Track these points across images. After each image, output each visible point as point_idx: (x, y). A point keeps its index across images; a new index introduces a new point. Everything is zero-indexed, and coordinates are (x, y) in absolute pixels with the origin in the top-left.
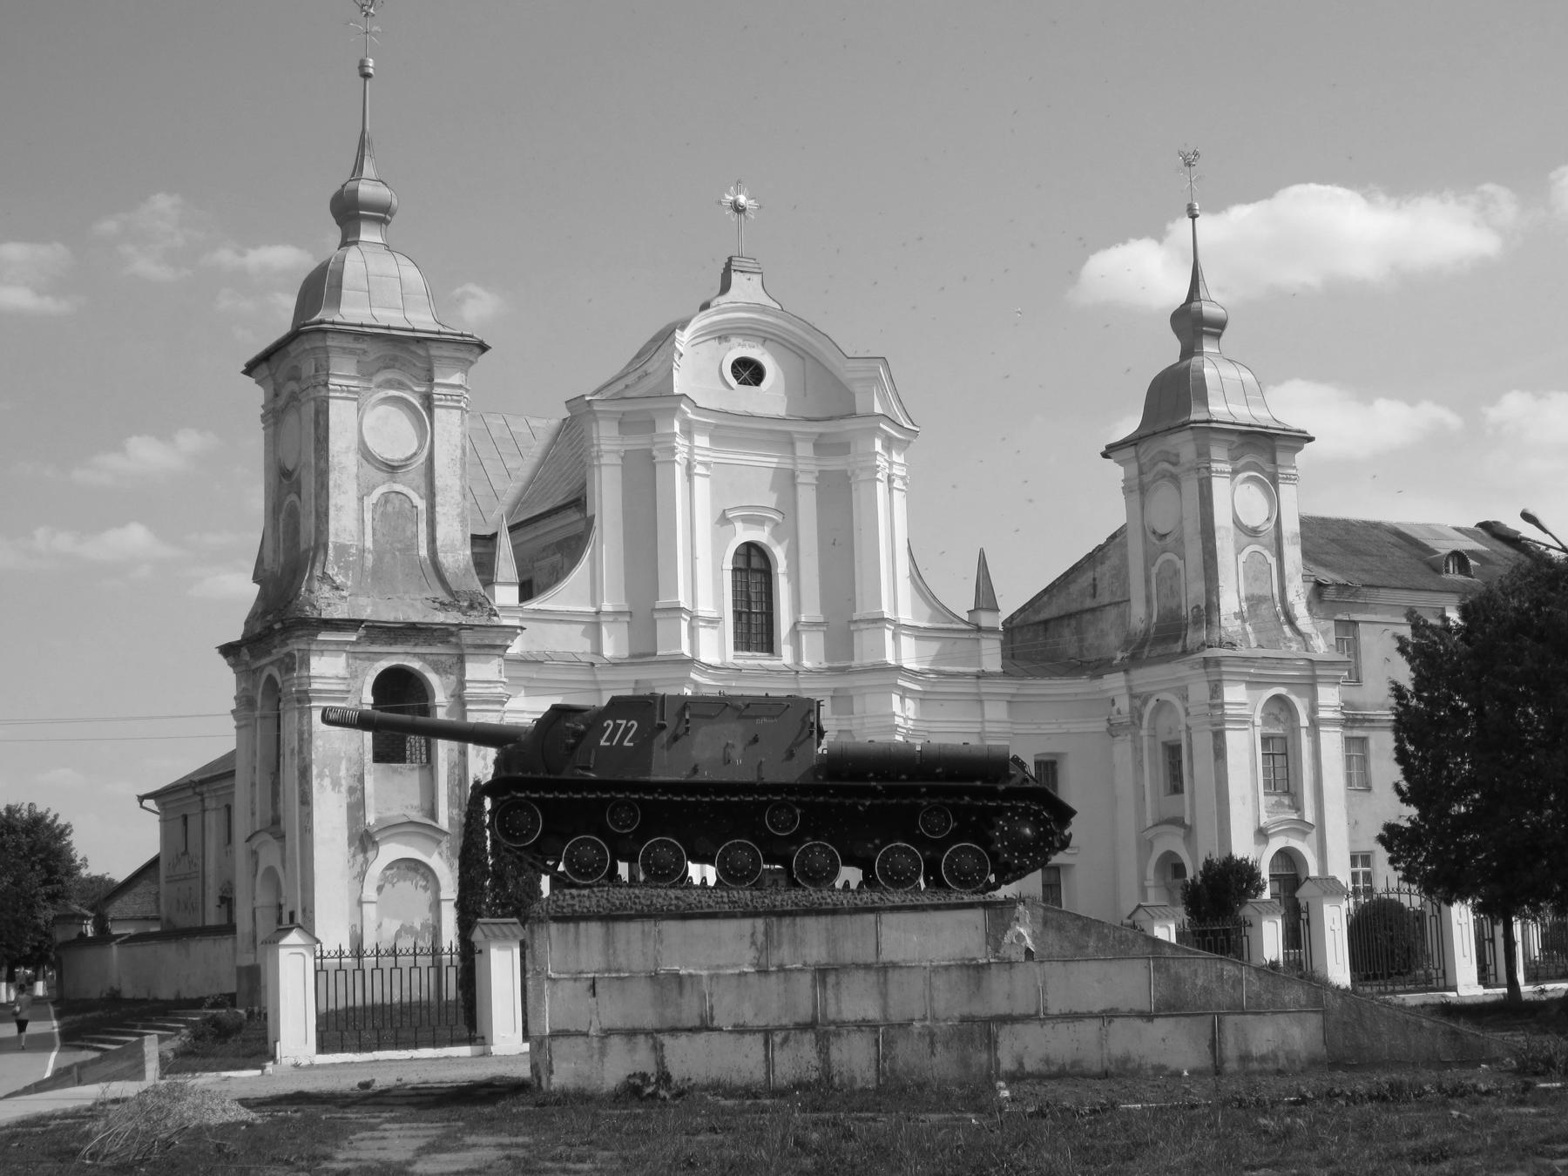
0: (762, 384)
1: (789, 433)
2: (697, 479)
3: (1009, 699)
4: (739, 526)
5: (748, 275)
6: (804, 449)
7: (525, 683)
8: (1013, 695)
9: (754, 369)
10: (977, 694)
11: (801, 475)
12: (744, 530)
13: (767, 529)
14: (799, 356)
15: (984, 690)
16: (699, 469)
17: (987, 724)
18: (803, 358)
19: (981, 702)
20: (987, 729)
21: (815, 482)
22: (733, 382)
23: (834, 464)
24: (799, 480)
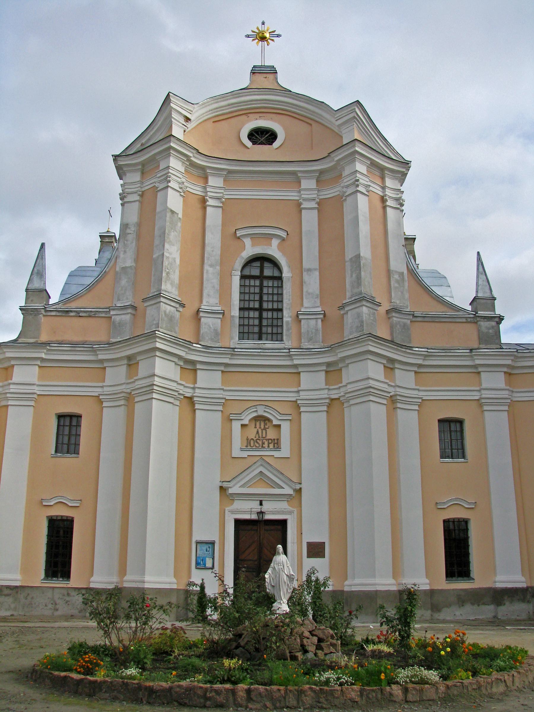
0: (274, 144)
1: (294, 173)
2: (209, 209)
3: (505, 370)
4: (247, 242)
5: (265, 75)
6: (309, 184)
7: (39, 363)
8: (513, 367)
9: (270, 136)
10: (476, 366)
11: (304, 202)
12: (253, 245)
13: (275, 242)
14: (307, 123)
15: (477, 362)
16: (210, 202)
17: (483, 392)
18: (311, 125)
19: (479, 373)
20: (483, 396)
21: (316, 206)
22: (249, 144)
23: (330, 193)
24: (302, 206)
